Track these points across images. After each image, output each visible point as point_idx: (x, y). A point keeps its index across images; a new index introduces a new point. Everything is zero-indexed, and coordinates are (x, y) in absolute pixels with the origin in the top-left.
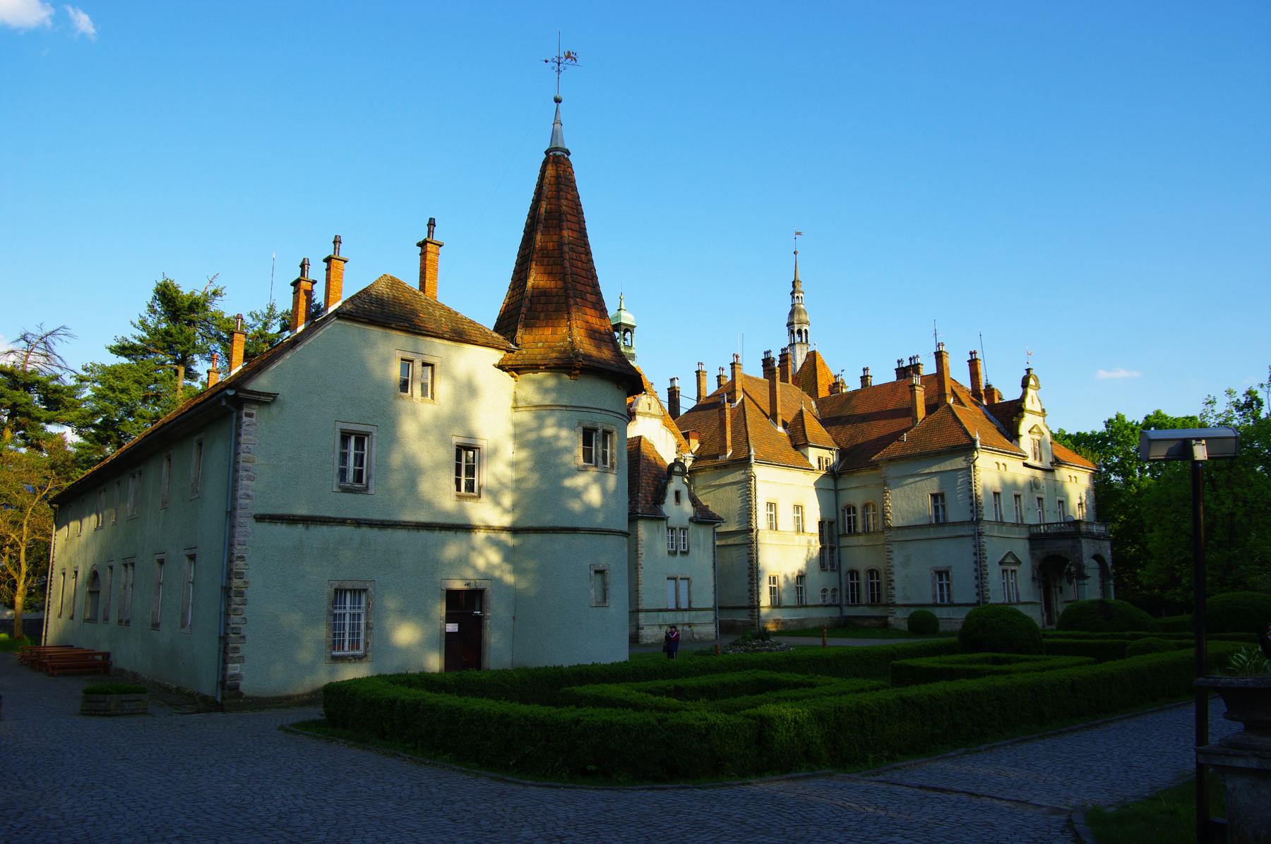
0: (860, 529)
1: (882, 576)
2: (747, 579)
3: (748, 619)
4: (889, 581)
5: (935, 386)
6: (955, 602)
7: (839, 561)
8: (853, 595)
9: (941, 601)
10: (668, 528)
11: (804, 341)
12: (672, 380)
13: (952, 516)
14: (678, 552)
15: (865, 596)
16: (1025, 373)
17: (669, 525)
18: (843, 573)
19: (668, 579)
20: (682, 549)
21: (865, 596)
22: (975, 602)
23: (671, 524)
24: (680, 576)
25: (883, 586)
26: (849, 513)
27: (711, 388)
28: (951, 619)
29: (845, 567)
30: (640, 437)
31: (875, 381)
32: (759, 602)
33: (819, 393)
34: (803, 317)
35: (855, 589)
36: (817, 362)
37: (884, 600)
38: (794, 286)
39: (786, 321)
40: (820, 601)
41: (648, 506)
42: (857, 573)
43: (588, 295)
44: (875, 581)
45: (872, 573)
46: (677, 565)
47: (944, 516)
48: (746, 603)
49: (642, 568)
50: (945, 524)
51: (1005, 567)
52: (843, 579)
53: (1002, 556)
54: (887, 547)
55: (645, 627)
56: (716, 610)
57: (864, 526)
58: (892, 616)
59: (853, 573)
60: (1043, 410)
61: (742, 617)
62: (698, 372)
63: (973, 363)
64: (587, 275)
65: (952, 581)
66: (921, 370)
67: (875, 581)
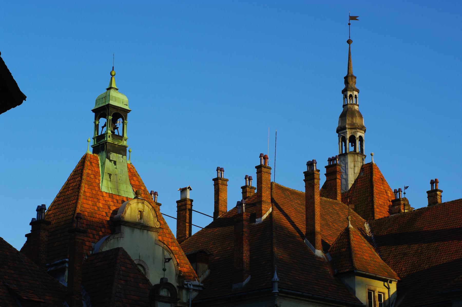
11: (358, 150)
12: (183, 190)
33: (375, 215)
34: (357, 120)
36: (374, 177)
38: (346, 82)
39: (336, 125)
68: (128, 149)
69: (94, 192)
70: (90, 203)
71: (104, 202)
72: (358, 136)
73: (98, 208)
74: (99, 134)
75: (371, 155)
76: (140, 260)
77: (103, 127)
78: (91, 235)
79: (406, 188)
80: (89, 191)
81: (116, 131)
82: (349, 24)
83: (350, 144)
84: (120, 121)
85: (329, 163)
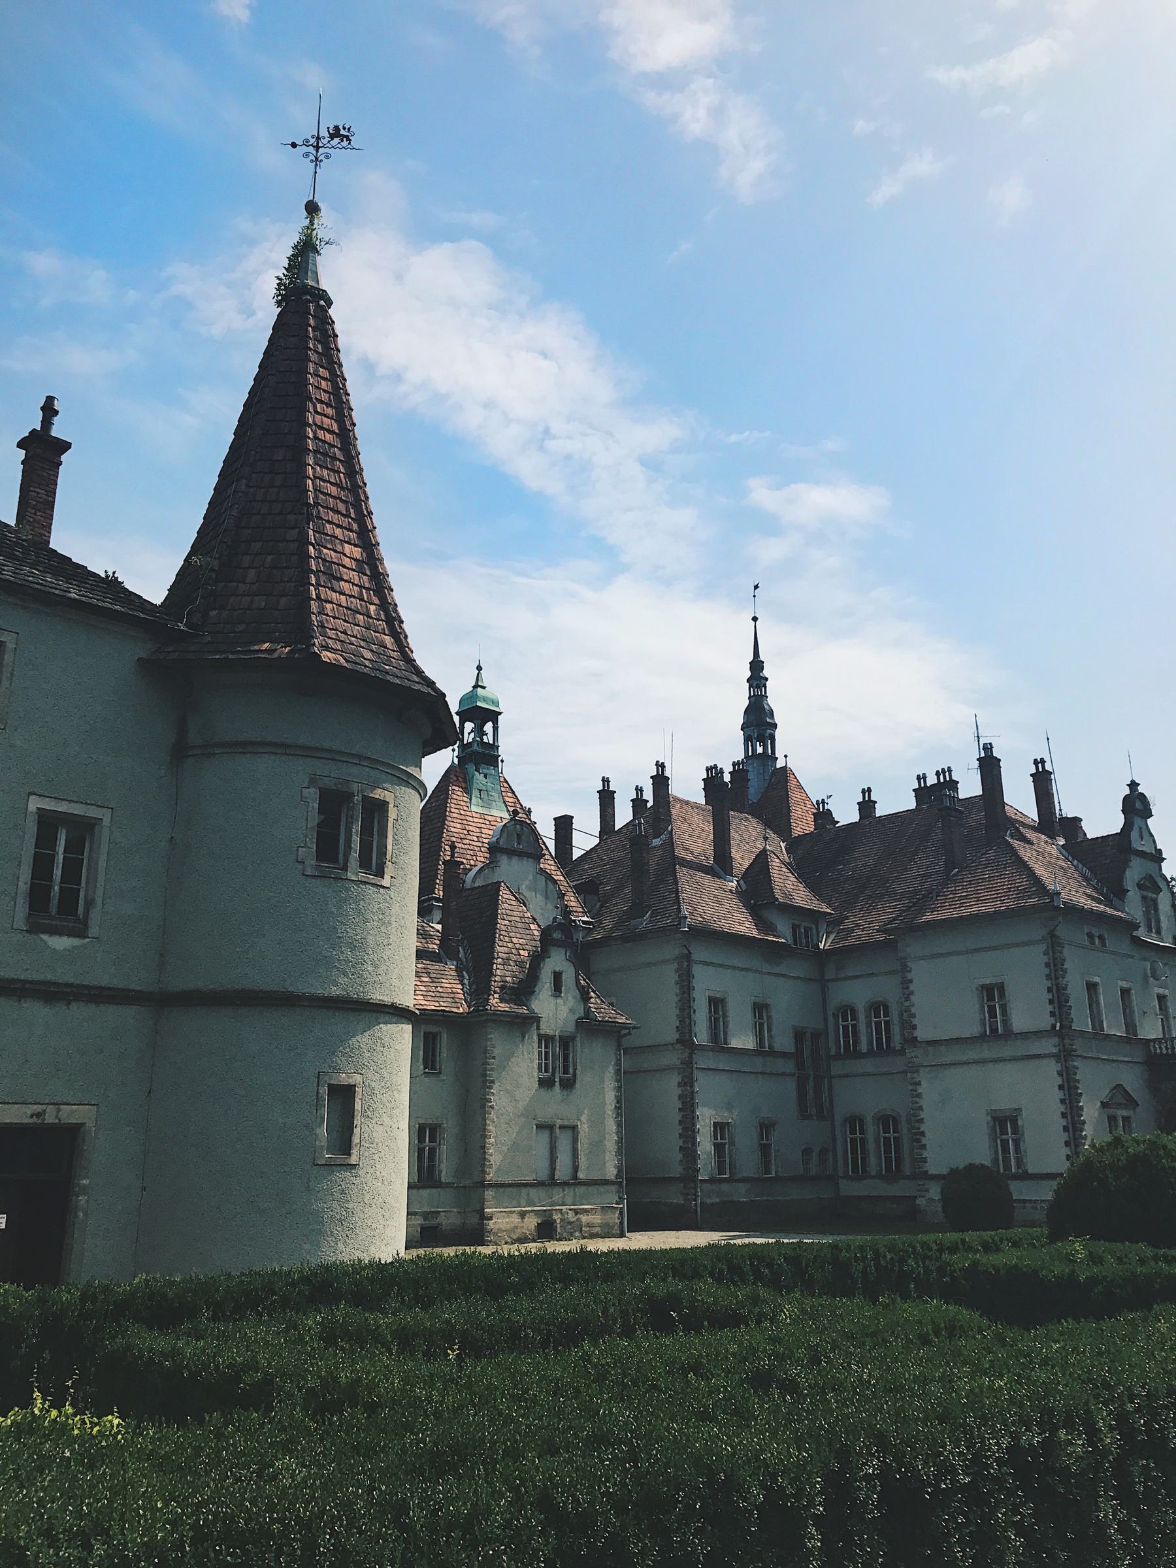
0: (864, 1047)
1: (904, 1127)
2: (679, 1130)
3: (678, 1200)
4: (915, 1134)
5: (978, 817)
6: (1031, 1170)
7: (831, 1101)
8: (855, 1161)
9: (1005, 1170)
10: (540, 1037)
13: (1020, 1021)
17: (542, 1032)
18: (838, 1119)
23: (545, 1029)
24: (559, 1122)
26: (845, 1019)
27: (623, 815)
28: (1024, 1201)
31: (880, 811)
43: (346, 545)
44: (891, 1135)
45: (887, 1121)
47: (1005, 1023)
49: (492, 1107)
50: (1009, 1035)
51: (1111, 1111)
54: (909, 1075)
58: (923, 1197)
59: (855, 1122)
61: (673, 1195)
63: (1042, 780)
65: (1023, 1135)
67: (891, 1135)
68: (500, 759)
69: (462, 812)
70: (458, 826)
72: (767, 735)
73: (468, 831)
74: (465, 742)
75: (786, 756)
77: (469, 734)
80: (457, 811)
81: (485, 737)
82: (754, 596)
83: (758, 743)
85: (734, 768)
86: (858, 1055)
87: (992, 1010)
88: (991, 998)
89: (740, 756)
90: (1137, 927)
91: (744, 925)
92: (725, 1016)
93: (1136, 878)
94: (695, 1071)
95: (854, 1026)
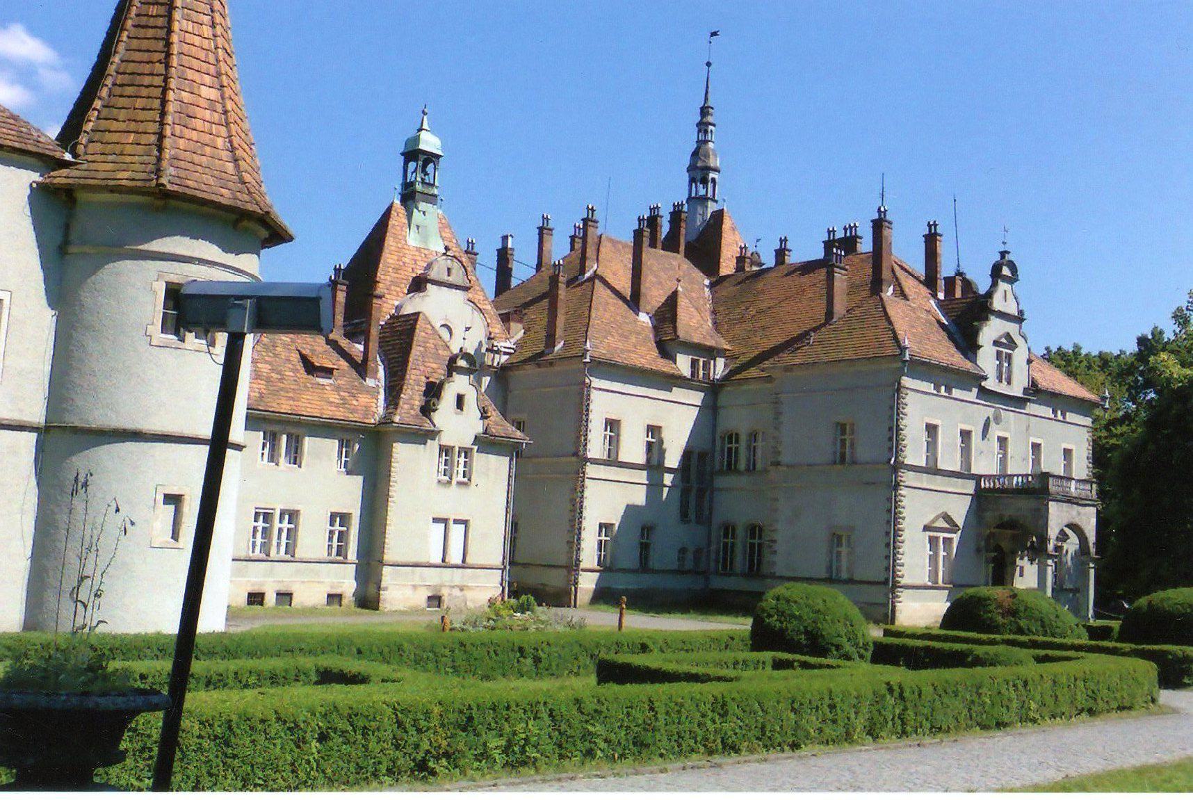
0: (742, 466)
4: (769, 541)
6: (857, 577)
7: (711, 509)
8: (725, 559)
11: (710, 194)
12: (505, 238)
14: (454, 482)
15: (740, 562)
16: (998, 257)
17: (443, 443)
18: (714, 527)
19: (436, 520)
20: (460, 478)
21: (740, 562)
22: (882, 579)
23: (446, 439)
24: (452, 517)
25: (766, 552)
26: (730, 442)
27: (559, 249)
29: (718, 519)
30: (417, 314)
32: (578, 561)
35: (728, 550)
37: (765, 569)
40: (675, 567)
41: (412, 412)
42: (734, 529)
44: (756, 541)
45: (755, 530)
46: (452, 502)
48: (563, 560)
52: (713, 539)
53: (932, 517)
55: (390, 588)
56: (505, 567)
57: (748, 465)
59: (729, 529)
60: (1021, 312)
62: (541, 229)
63: (931, 240)
64: (207, 56)
66: (858, 245)
69: (400, 246)
71: (411, 257)
73: (404, 263)
76: (447, 320)
78: (395, 293)
79: (758, 240)
80: (394, 244)
83: (701, 186)
84: (431, 166)
86: (737, 471)
87: (843, 441)
88: (843, 432)
89: (681, 196)
90: (985, 378)
91: (647, 357)
92: (618, 435)
93: (995, 336)
94: (586, 480)
95: (737, 449)
